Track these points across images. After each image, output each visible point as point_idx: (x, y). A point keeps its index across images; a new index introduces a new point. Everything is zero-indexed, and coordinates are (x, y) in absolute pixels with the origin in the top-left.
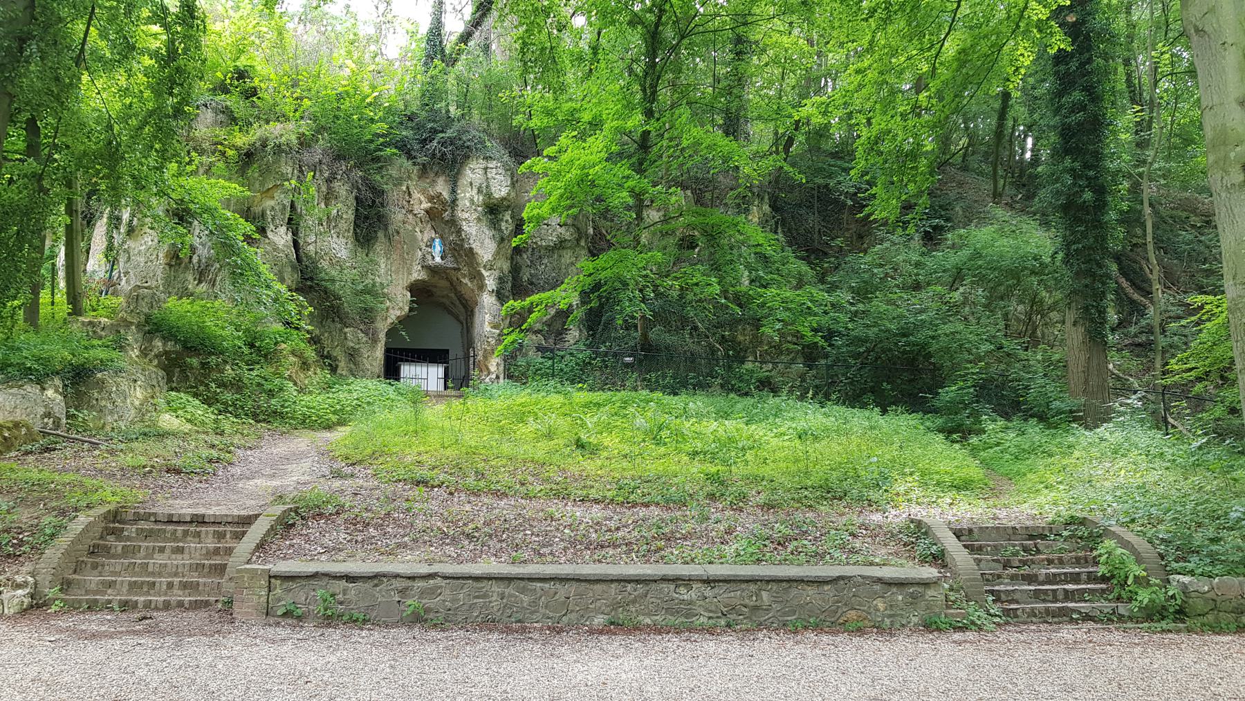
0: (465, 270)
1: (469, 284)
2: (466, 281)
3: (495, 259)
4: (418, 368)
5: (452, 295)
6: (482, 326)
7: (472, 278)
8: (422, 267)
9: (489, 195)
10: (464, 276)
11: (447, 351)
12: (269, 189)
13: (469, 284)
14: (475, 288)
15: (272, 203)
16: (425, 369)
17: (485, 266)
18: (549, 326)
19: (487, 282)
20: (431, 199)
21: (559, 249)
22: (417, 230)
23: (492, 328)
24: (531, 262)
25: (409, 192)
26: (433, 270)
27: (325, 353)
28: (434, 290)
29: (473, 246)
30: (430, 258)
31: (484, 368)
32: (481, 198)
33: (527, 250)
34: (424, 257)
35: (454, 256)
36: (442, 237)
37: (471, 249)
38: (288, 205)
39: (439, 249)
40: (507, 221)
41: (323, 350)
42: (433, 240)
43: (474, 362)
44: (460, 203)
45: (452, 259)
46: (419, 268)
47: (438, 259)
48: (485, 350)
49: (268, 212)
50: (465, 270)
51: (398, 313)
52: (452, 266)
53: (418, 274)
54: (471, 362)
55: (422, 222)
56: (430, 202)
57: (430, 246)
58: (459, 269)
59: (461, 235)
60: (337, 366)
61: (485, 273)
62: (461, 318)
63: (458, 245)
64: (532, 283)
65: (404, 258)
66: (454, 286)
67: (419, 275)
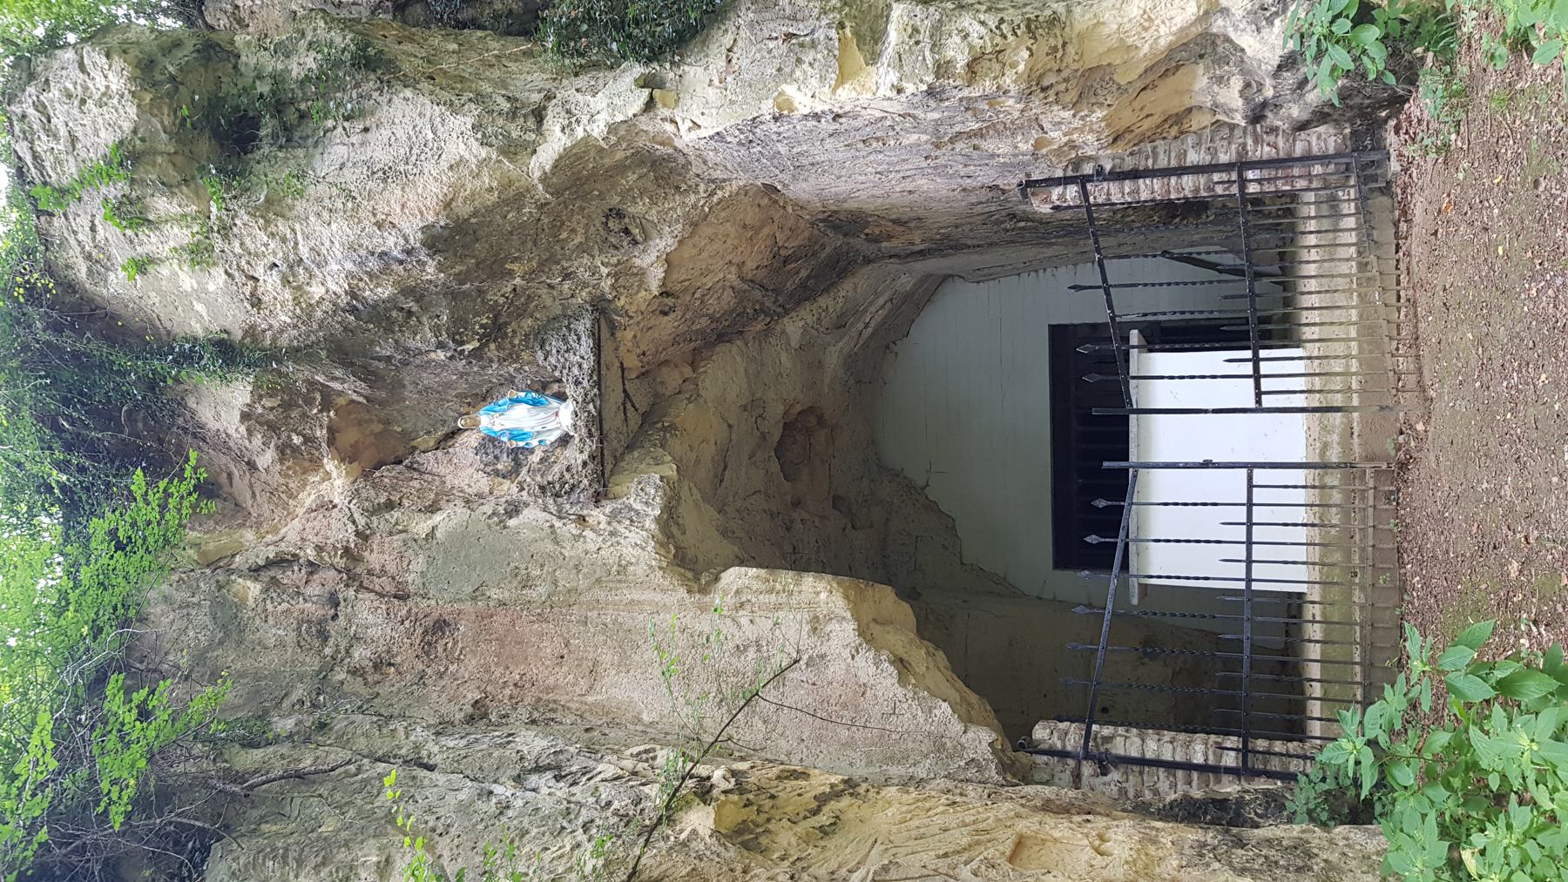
1: (663, 243)
2: (650, 260)
3: (479, 98)
5: (793, 327)
8: (598, 499)
9: (129, 156)
10: (626, 275)
11: (1061, 337)
13: (663, 243)
14: (678, 206)
17: (514, 149)
19: (598, 130)
20: (299, 458)
22: (421, 526)
23: (873, 58)
25: (270, 564)
28: (776, 410)
29: (412, 228)
31: (1163, 100)
32: (162, 205)
35: (539, 338)
36: (482, 397)
37: (443, 240)
39: (522, 410)
43: (1119, 176)
44: (233, 318)
45: (554, 344)
46: (597, 516)
47: (564, 417)
51: (844, 632)
52: (585, 347)
54: (1118, 193)
55: (390, 506)
56: (316, 464)
57: (518, 456)
61: (554, 143)
62: (906, 282)
65: (549, 602)
67: (635, 519)
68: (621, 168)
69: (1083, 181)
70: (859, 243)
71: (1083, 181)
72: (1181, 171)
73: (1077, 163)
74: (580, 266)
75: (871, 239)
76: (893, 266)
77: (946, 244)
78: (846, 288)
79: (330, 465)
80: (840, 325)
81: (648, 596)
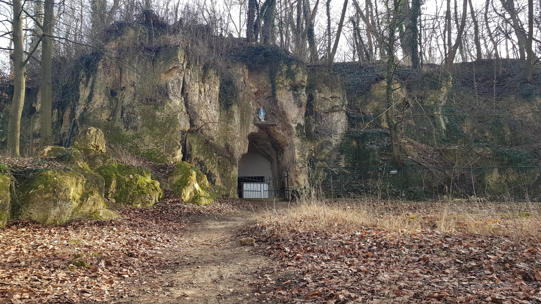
0: (280, 125)
1: (282, 134)
2: (280, 131)
4: (255, 185)
5: (269, 143)
6: (293, 156)
7: (284, 130)
8: (254, 124)
10: (279, 129)
11: (264, 177)
12: (170, 70)
13: (282, 134)
14: (286, 136)
15: (172, 79)
16: (259, 185)
18: (329, 156)
21: (331, 112)
22: (251, 103)
24: (316, 120)
26: (261, 127)
27: (207, 171)
30: (258, 120)
33: (313, 114)
34: (255, 120)
38: (182, 80)
39: (263, 113)
40: (304, 95)
41: (206, 170)
42: (259, 109)
47: (263, 120)
48: (297, 171)
49: (170, 84)
50: (280, 125)
52: (271, 123)
53: (253, 129)
56: (257, 88)
58: (275, 125)
59: (277, 104)
60: (215, 180)
62: (273, 157)
63: (274, 111)
64: (317, 133)
66: (270, 136)
68: (290, 131)
69: (287, 176)
70: (280, 152)
71: (287, 176)
72: (288, 185)
73: (289, 176)
74: (280, 124)
75: (280, 154)
76: (275, 156)
77: (279, 163)
78: (273, 150)
79: (256, 89)
80: (268, 149)
81: (245, 131)
